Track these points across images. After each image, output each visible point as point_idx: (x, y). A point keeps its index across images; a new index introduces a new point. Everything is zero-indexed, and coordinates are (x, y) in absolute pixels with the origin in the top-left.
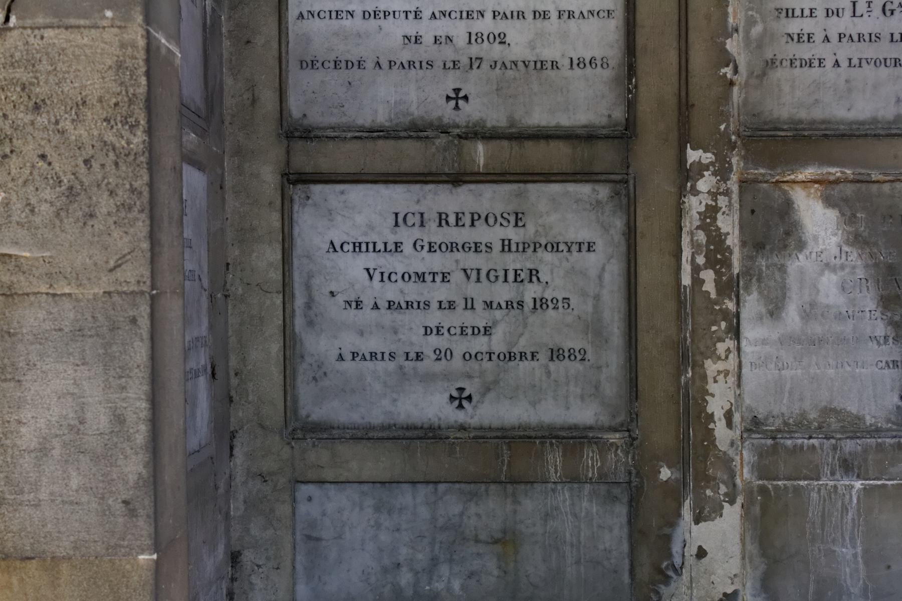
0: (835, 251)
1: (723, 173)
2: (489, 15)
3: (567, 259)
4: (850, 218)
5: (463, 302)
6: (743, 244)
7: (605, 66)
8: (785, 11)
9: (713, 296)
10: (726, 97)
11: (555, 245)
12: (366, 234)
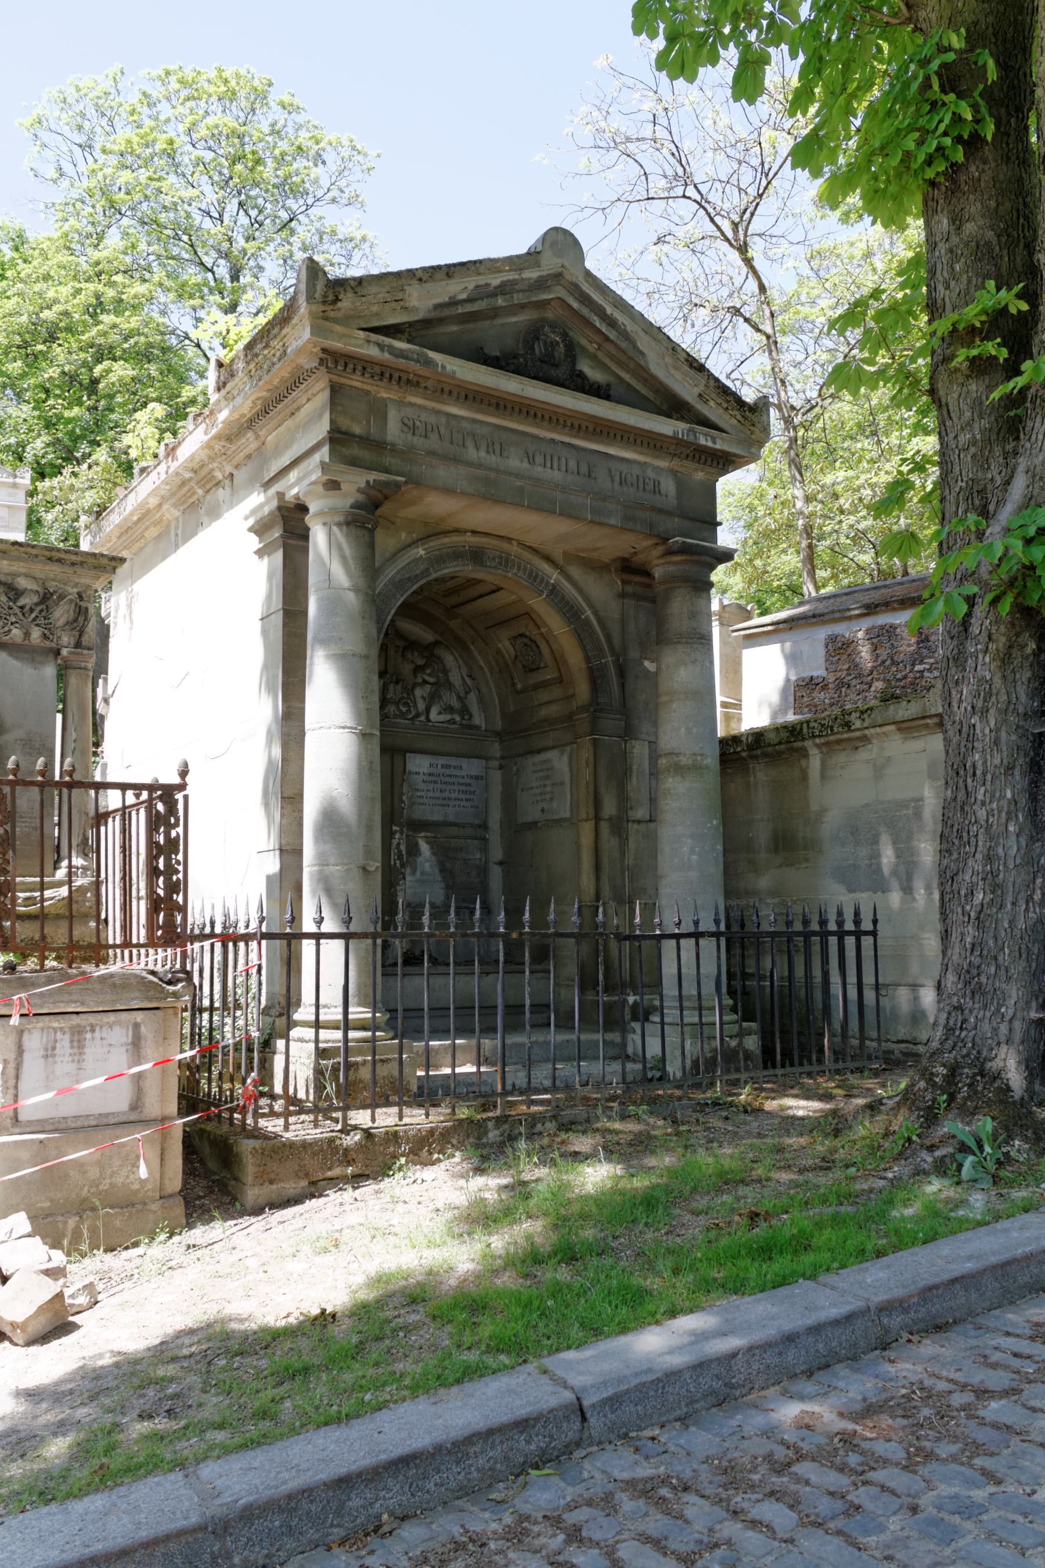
1: (402, 833)
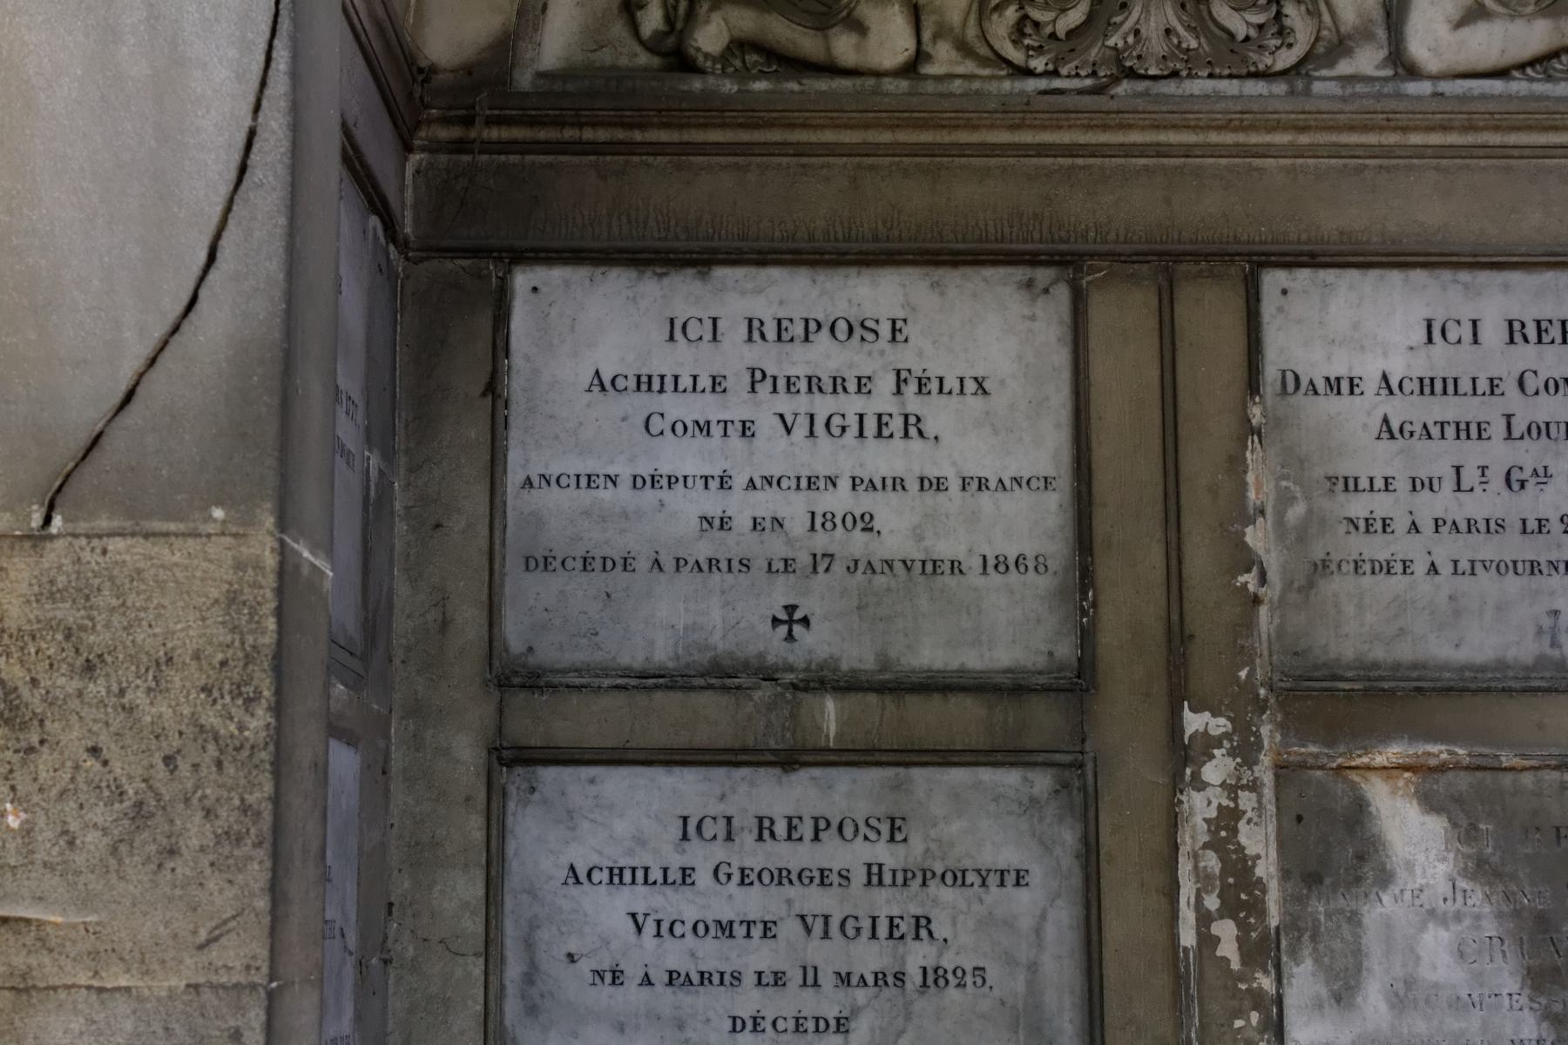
0: (1444, 888)
1: (1246, 752)
2: (844, 484)
3: (981, 900)
4: (1468, 832)
5: (801, 972)
6: (1285, 875)
7: (1041, 569)
8: (1341, 481)
9: (1235, 965)
10: (1248, 623)
11: (959, 875)
12: (630, 853)
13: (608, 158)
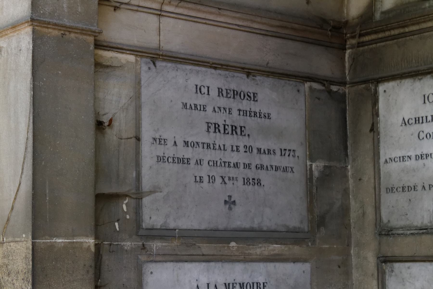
13: (400, 40)
